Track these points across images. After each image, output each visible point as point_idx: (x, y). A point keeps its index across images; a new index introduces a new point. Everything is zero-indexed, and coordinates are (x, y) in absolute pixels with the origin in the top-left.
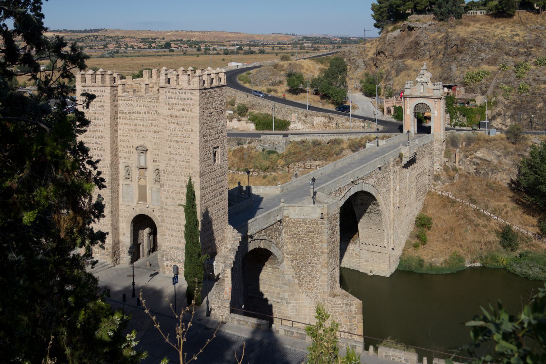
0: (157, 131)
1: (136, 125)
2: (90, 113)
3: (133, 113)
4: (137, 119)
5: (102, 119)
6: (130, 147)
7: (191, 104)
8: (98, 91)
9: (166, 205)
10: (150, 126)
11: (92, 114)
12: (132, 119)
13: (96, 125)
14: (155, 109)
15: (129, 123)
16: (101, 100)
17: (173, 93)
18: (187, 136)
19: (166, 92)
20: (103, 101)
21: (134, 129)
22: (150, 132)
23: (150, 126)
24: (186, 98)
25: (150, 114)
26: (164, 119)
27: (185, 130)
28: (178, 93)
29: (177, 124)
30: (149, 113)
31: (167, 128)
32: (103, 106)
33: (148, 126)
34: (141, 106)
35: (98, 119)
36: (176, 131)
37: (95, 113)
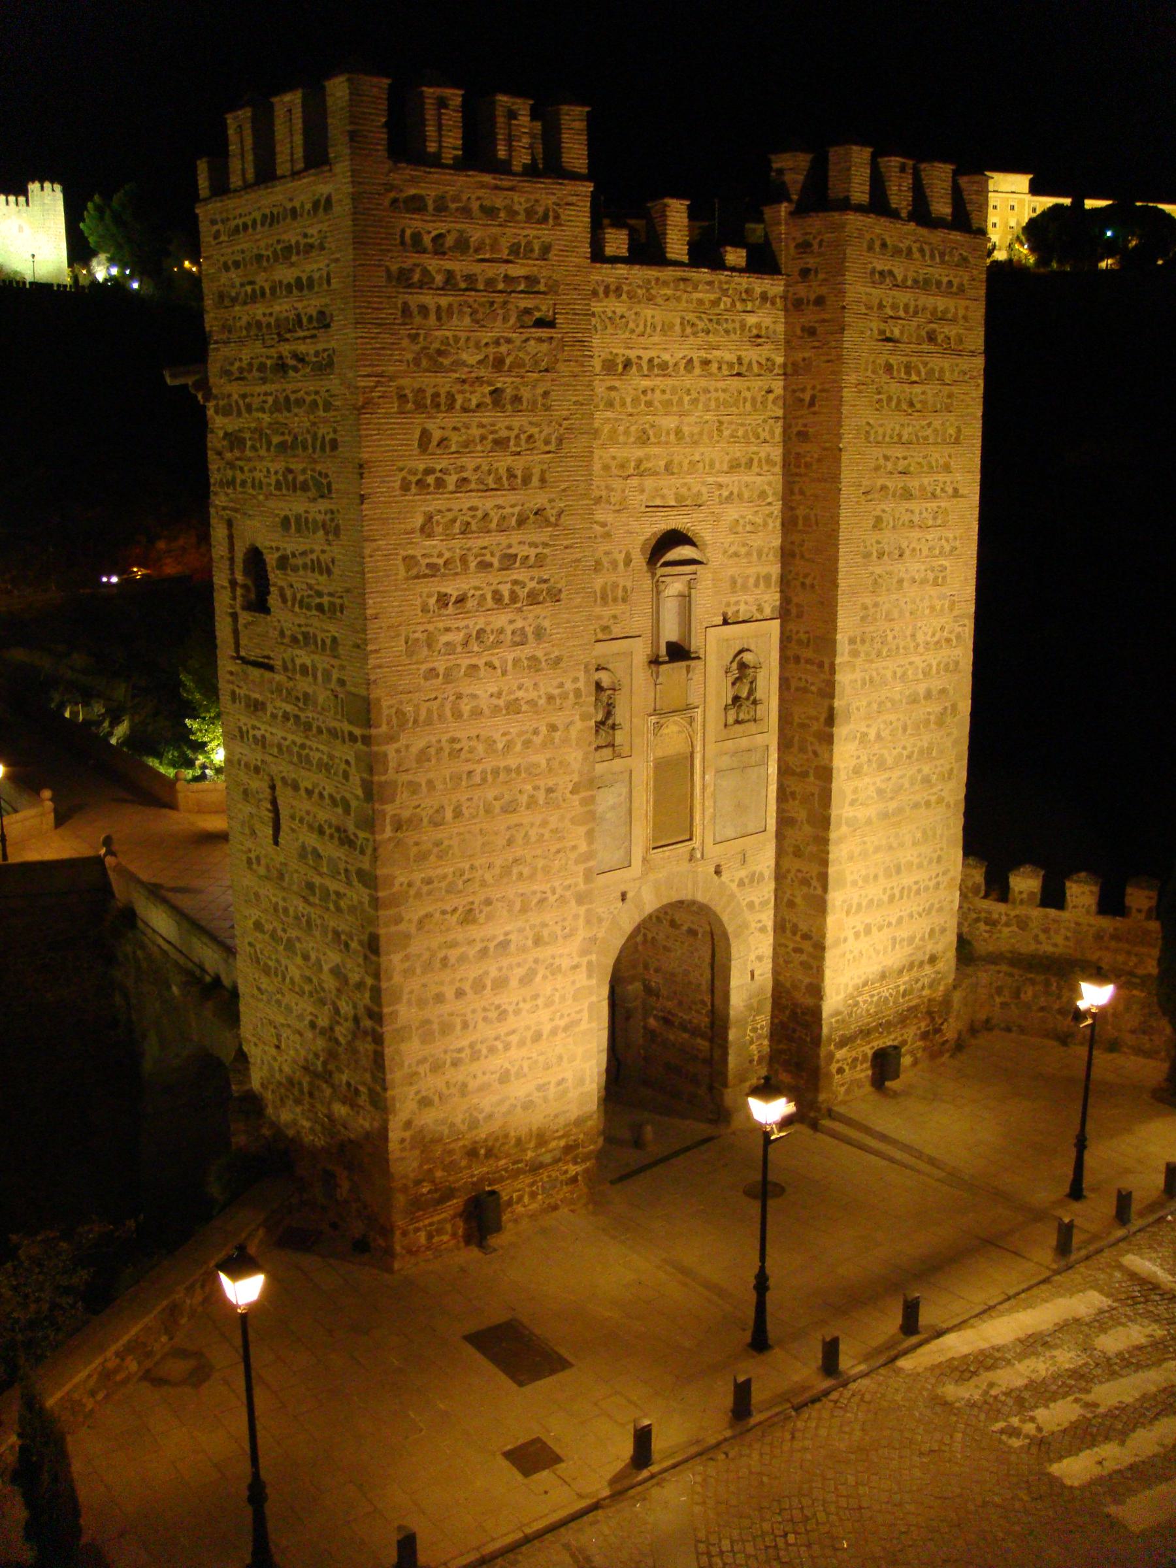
0: (743, 461)
6: (614, 564)
9: (852, 803)
13: (501, 443)
37: (499, 363)
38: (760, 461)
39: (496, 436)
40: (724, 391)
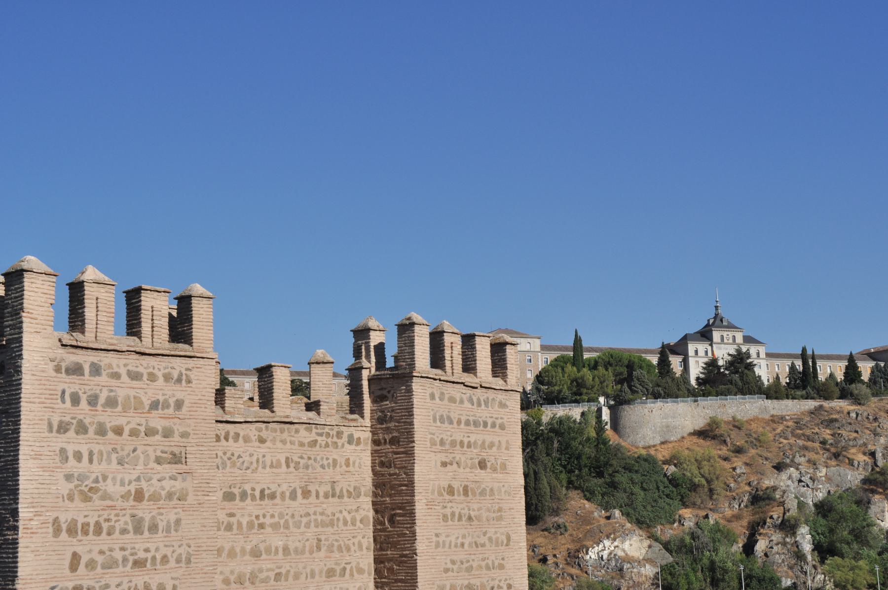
0: (338, 569)
1: (256, 553)
2: (105, 497)
3: (244, 496)
4: (262, 526)
5: (178, 522)
7: (504, 445)
8: (152, 377)
10: (311, 552)
11: (119, 503)
12: (240, 524)
13: (139, 564)
14: (329, 474)
15: (227, 546)
16: (167, 423)
17: (452, 400)
18: (496, 564)
19: (432, 396)
20: (178, 428)
21: (248, 569)
22: (313, 575)
23: (311, 552)
24: (490, 422)
25: (312, 498)
26: (429, 504)
27: (490, 539)
28: (467, 404)
29: (470, 518)
30: (306, 494)
31: (441, 539)
32: (176, 459)
33: (303, 552)
34: (279, 465)
35: (154, 528)
36: (466, 546)
37: (139, 496)
38: (351, 570)
39: (136, 557)
40: (322, 514)
